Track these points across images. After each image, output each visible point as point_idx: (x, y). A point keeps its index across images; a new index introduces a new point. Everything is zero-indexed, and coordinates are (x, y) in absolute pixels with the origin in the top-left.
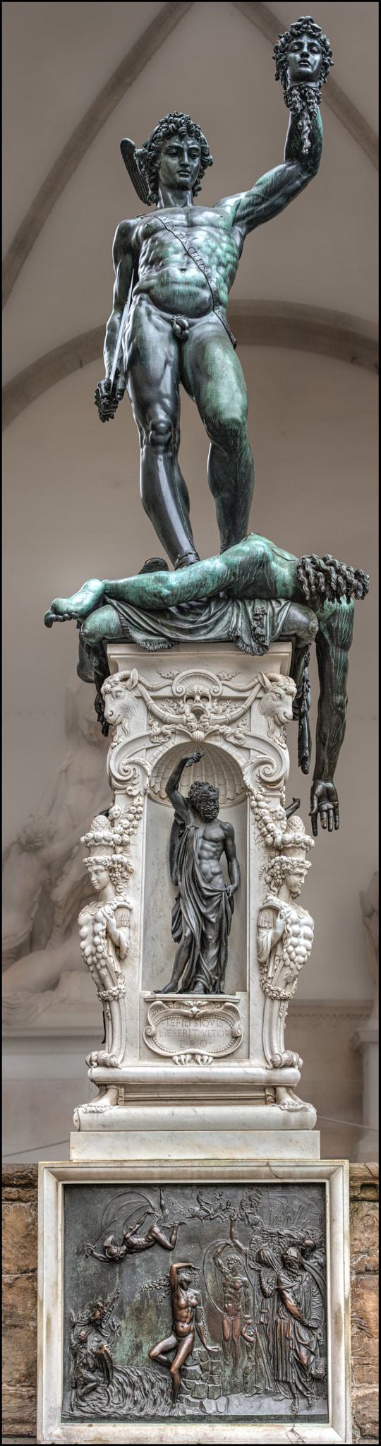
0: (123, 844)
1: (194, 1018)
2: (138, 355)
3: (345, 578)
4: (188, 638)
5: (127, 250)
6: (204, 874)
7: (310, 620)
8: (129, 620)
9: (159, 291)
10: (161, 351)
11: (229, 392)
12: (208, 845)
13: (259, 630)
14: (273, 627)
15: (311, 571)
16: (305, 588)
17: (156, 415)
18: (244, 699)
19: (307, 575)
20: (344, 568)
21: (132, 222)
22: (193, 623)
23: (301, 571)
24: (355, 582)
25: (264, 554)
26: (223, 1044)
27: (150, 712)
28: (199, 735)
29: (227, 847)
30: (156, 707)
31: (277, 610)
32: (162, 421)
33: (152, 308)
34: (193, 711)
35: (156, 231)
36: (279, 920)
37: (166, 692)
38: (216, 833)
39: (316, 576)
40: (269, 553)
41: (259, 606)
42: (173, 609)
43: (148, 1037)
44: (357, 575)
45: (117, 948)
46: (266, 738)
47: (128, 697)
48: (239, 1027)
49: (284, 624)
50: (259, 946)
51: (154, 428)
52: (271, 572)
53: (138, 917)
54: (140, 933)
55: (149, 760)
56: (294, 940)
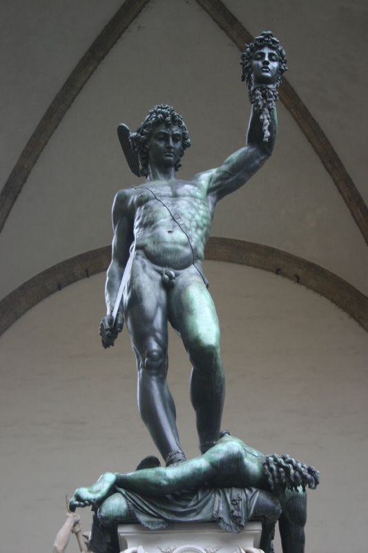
2: (136, 297)
3: (301, 473)
5: (125, 215)
7: (276, 504)
8: (136, 506)
9: (151, 247)
10: (152, 297)
11: (206, 324)
13: (236, 513)
15: (274, 467)
16: (270, 480)
17: (151, 345)
19: (271, 470)
20: (299, 465)
21: (127, 191)
22: (184, 507)
23: (266, 467)
24: (309, 476)
25: (239, 453)
31: (249, 497)
32: (155, 350)
33: (146, 262)
35: (147, 200)
39: (278, 471)
40: (243, 452)
41: (236, 493)
42: (169, 496)
44: (310, 471)
49: (255, 508)
51: (150, 355)
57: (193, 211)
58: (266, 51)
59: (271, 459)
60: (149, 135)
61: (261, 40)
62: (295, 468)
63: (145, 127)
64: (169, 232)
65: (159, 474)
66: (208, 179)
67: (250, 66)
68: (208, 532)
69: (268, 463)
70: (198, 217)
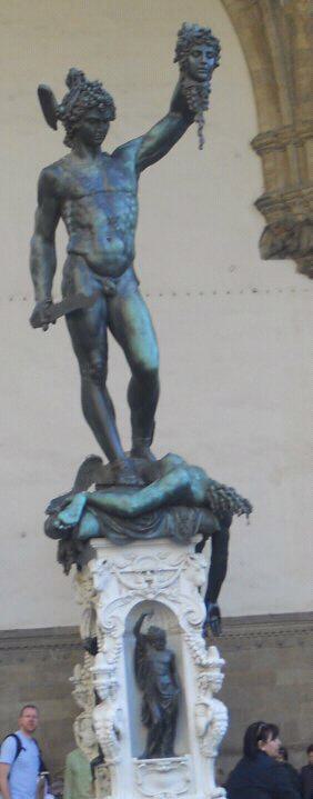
0: (115, 669)
1: (164, 772)
4: (139, 536)
6: (162, 684)
9: (94, 258)
12: (162, 666)
14: (194, 528)
16: (212, 506)
18: (175, 571)
22: (143, 525)
26: (181, 786)
27: (119, 582)
28: (151, 597)
29: (172, 667)
30: (124, 579)
33: (88, 273)
34: (147, 581)
35: (82, 197)
36: (210, 713)
37: (128, 569)
38: (167, 658)
43: (139, 785)
45: (118, 734)
46: (188, 594)
47: (107, 574)
48: (188, 775)
50: (196, 727)
51: (93, 367)
52: (192, 494)
53: (125, 713)
54: (127, 724)
55: (123, 613)
56: (219, 723)
57: (127, 211)
58: (205, 49)
59: (213, 488)
60: (80, 117)
61: (199, 37)
62: (234, 500)
63: (75, 107)
64: (109, 240)
65: (125, 502)
66: (133, 157)
67: (187, 60)
68: (161, 542)
69: (209, 490)
70: (131, 217)
